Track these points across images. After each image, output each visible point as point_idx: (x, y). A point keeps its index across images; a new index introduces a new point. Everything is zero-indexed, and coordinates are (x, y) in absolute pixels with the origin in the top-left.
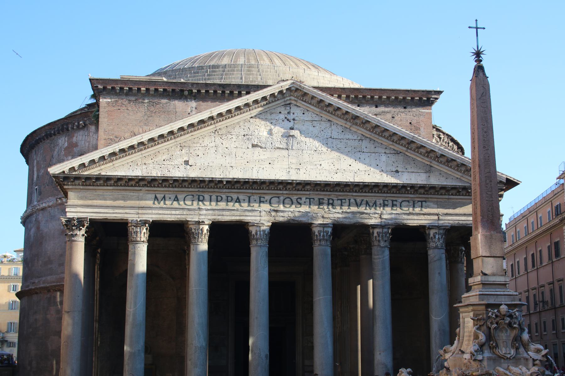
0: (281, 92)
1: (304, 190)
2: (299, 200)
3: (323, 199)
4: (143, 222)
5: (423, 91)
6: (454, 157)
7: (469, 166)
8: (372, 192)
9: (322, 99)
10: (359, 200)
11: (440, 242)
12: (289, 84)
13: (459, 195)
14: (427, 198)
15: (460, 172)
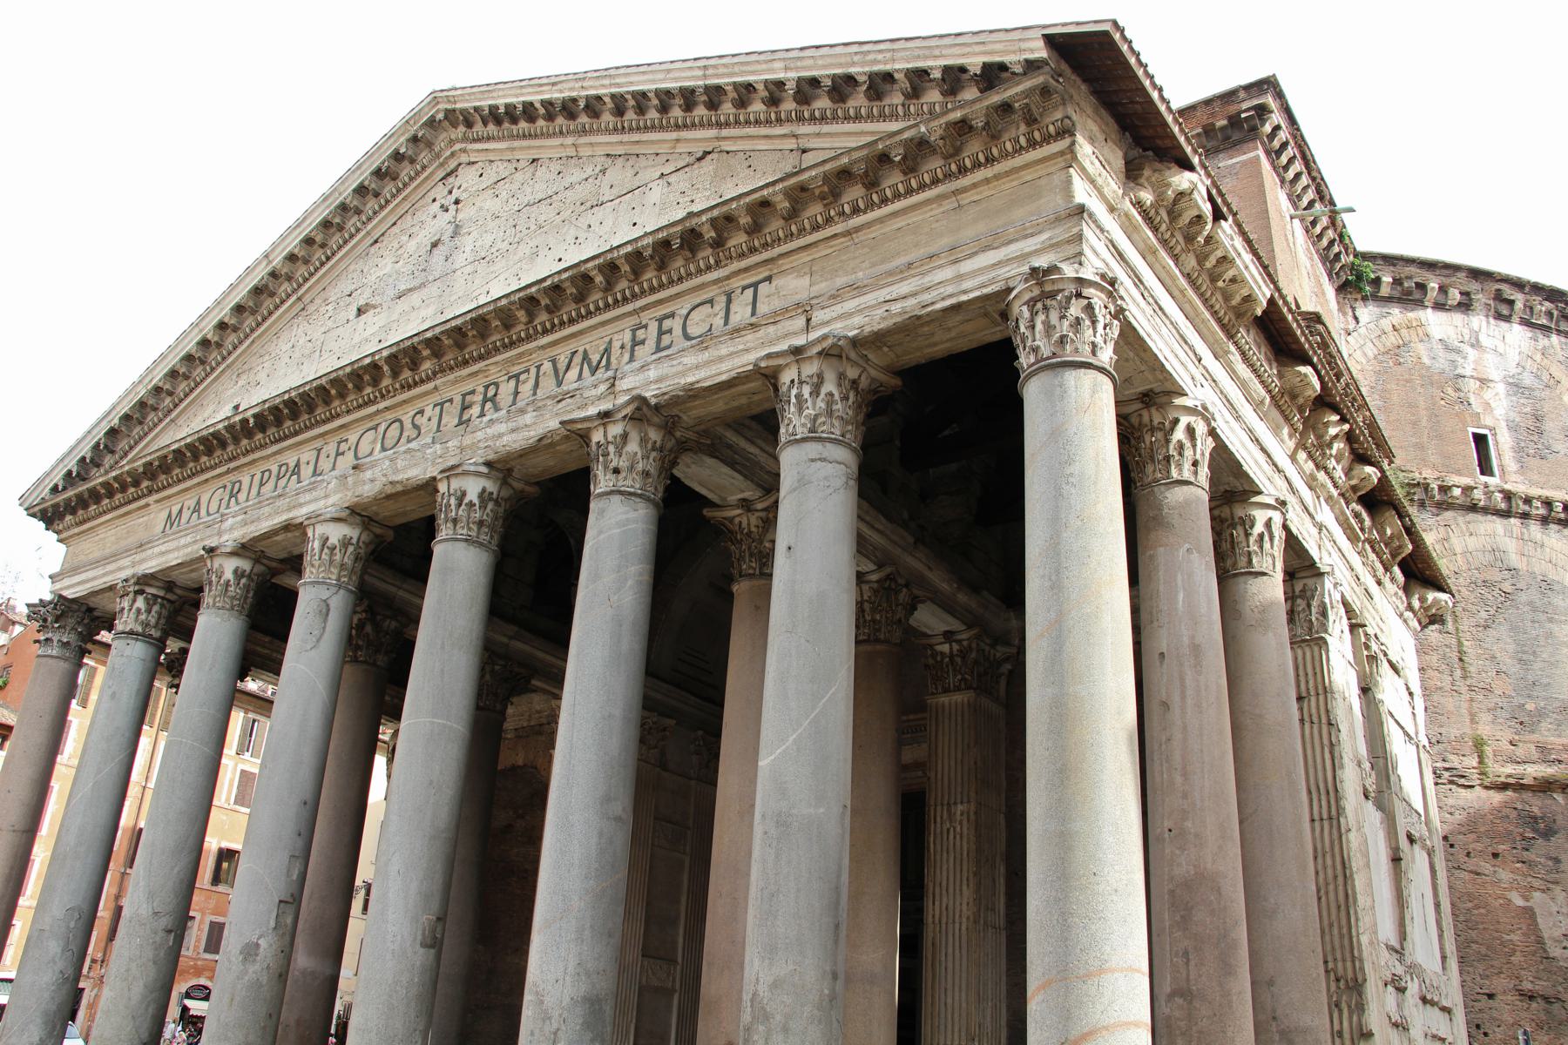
0: (415, 139)
1: (422, 381)
2: (418, 419)
3: (473, 392)
4: (132, 581)
5: (1208, 102)
6: (841, 65)
7: (897, 71)
8: (589, 314)
9: (490, 102)
10: (562, 362)
11: (806, 412)
12: (426, 110)
13: (885, 201)
14: (766, 262)
15: (894, 116)
